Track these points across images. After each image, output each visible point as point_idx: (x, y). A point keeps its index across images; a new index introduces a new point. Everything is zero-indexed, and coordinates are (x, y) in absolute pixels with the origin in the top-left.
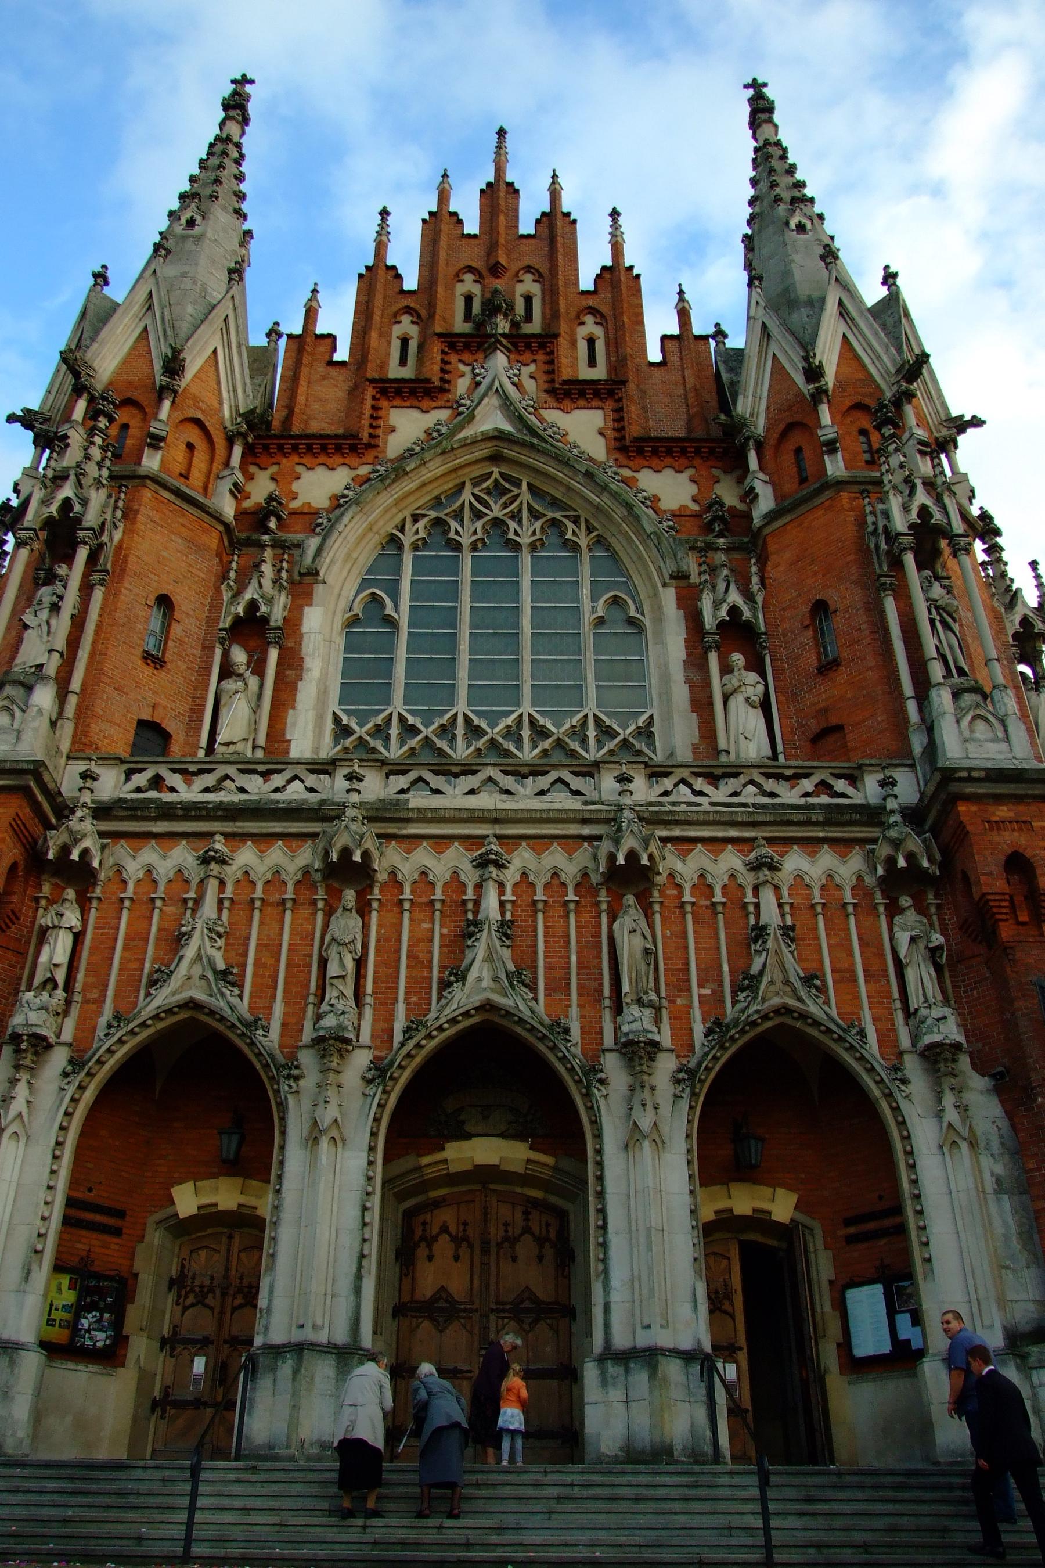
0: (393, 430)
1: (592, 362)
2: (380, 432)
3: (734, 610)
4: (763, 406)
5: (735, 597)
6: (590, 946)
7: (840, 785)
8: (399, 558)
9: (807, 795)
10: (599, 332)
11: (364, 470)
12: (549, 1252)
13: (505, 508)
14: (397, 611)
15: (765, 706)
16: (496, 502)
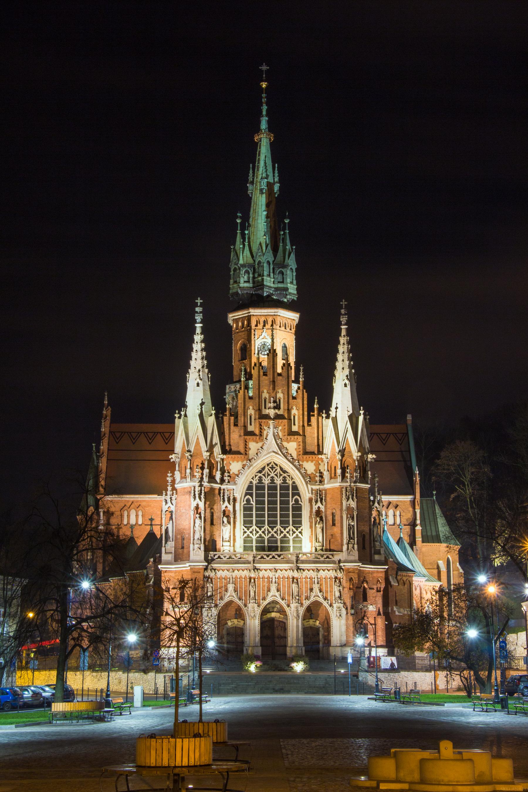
0: (250, 449)
1: (294, 424)
2: (247, 450)
3: (319, 507)
4: (330, 451)
5: (319, 504)
6: (289, 587)
7: (331, 556)
8: (252, 486)
9: (325, 558)
10: (297, 414)
11: (245, 462)
12: (282, 629)
13: (274, 472)
14: (253, 501)
15: (323, 530)
16: (272, 470)
